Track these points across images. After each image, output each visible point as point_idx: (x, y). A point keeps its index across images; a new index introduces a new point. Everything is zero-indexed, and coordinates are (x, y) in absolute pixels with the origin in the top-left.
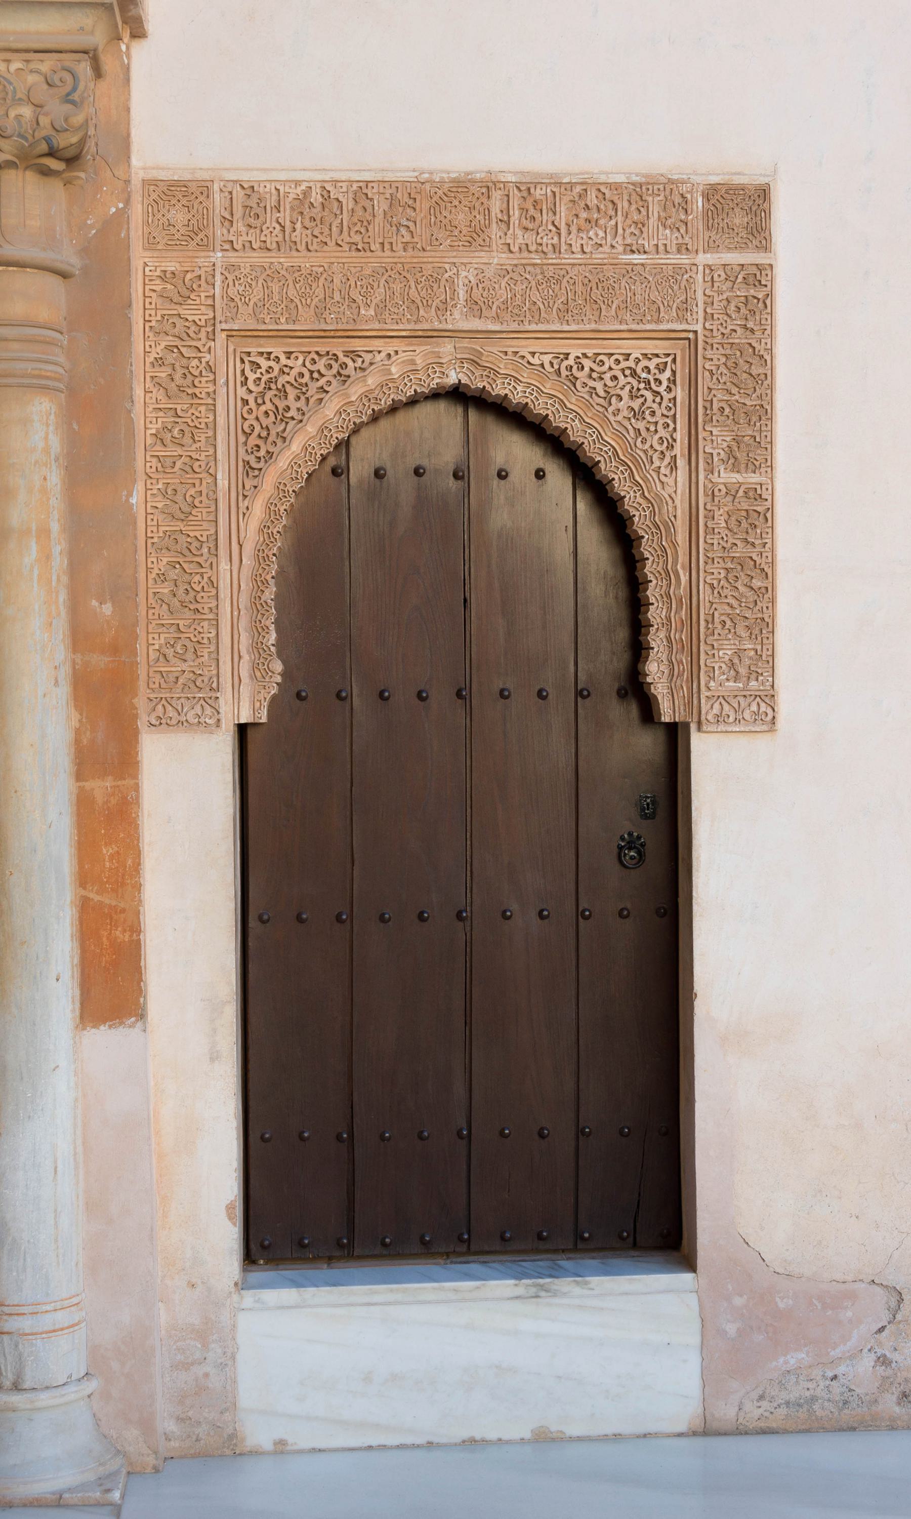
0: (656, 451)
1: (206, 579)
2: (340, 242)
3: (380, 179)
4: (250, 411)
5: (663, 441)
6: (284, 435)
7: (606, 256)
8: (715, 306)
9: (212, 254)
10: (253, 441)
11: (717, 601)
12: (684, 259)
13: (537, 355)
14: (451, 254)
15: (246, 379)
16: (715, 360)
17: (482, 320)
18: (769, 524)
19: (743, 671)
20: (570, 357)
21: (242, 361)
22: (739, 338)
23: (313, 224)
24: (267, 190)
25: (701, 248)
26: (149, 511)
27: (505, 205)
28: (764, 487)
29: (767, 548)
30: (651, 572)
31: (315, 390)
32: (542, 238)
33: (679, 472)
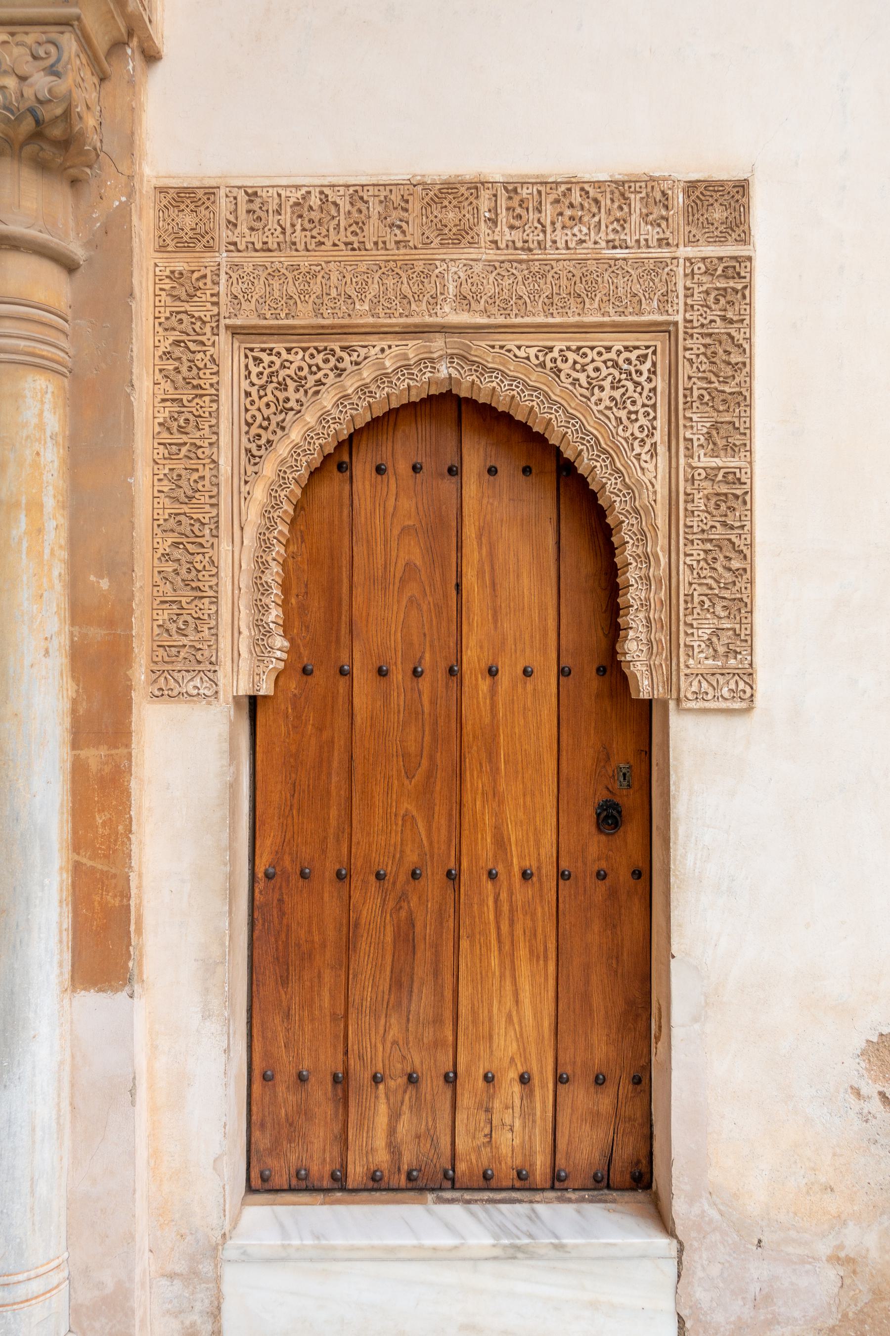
0: (636, 438)
2: (337, 242)
3: (375, 182)
4: (252, 403)
6: (284, 424)
7: (590, 251)
8: (695, 298)
9: (217, 254)
10: (254, 430)
11: (696, 581)
12: (665, 253)
13: (523, 348)
14: (441, 251)
15: (250, 373)
16: (695, 349)
17: (471, 313)
18: (748, 507)
19: (721, 650)
20: (554, 349)
21: (246, 357)
22: (719, 327)
23: (312, 226)
24: (270, 194)
25: (681, 242)
27: (493, 204)
28: (743, 471)
29: (746, 531)
31: (313, 383)
32: (528, 235)
33: (658, 458)
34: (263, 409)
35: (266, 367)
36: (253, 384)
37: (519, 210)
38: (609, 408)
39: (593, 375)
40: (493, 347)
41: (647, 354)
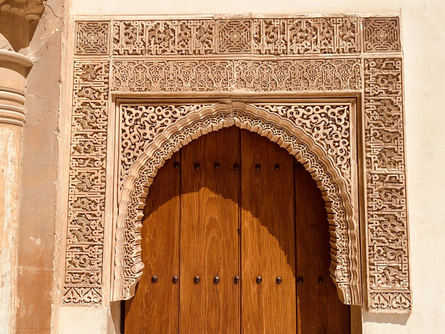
0: (339, 156)
1: (98, 223)
2: (173, 50)
3: (195, 18)
4: (126, 135)
5: (343, 151)
6: (143, 148)
7: (311, 55)
8: (371, 80)
9: (108, 56)
10: (127, 151)
11: (375, 238)
12: (353, 56)
13: (274, 107)
14: (230, 55)
15: (125, 119)
16: (371, 108)
17: (246, 88)
18: (404, 196)
19: (391, 279)
21: (123, 110)
22: (384, 96)
23: (160, 41)
24: (137, 25)
25: (362, 50)
26: (71, 186)
27: (258, 30)
28: (400, 176)
29: (403, 210)
30: (337, 221)
31: (160, 125)
32: (277, 47)
33: (351, 167)
34: (132, 139)
35: (134, 116)
36: (126, 125)
37: (272, 33)
38: (322, 139)
39: (314, 121)
40: (258, 106)
41: (344, 110)
